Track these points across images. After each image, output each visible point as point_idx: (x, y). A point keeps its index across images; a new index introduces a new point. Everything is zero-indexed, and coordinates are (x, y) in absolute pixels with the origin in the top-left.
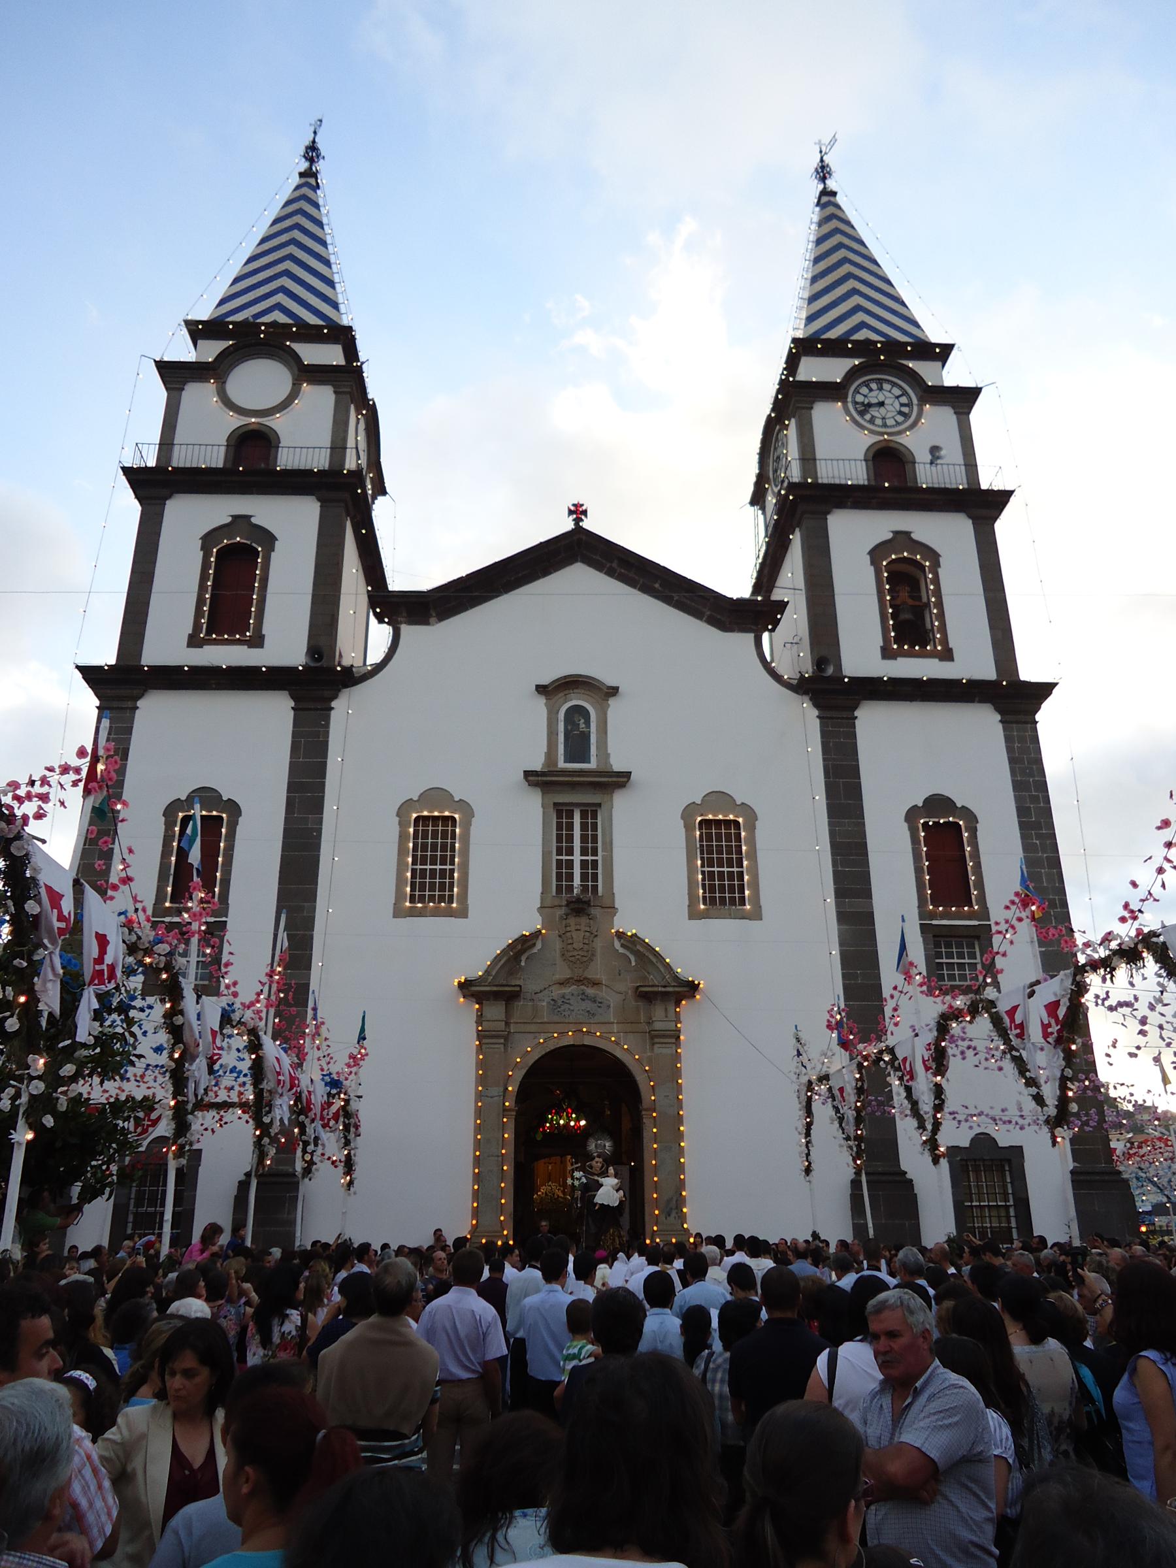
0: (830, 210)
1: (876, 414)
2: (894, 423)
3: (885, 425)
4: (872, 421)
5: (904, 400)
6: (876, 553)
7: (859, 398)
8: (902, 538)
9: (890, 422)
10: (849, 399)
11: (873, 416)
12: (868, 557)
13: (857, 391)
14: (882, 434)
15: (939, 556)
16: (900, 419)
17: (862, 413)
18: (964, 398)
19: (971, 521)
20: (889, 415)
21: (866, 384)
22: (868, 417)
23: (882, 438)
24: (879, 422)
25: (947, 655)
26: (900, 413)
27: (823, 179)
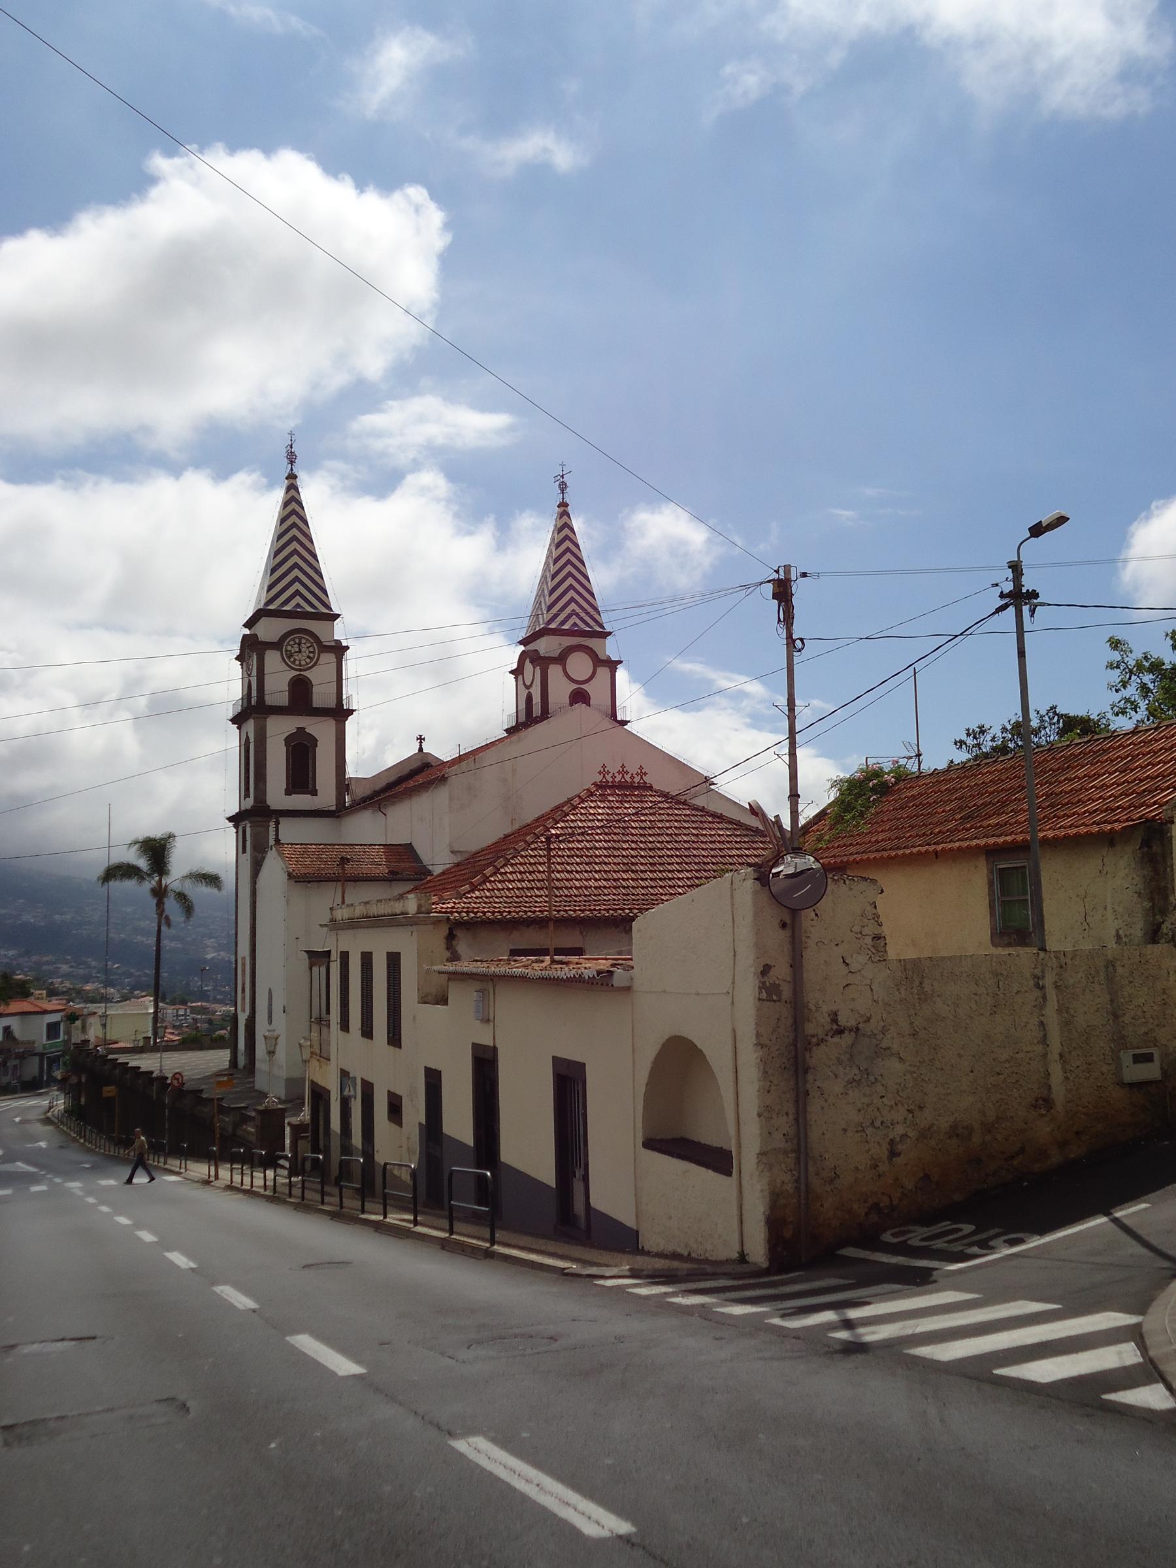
0: (293, 492)
1: (297, 658)
2: (305, 663)
3: (300, 665)
4: (294, 662)
5: (311, 649)
6: (288, 740)
7: (289, 648)
8: (301, 730)
9: (303, 663)
10: (284, 650)
11: (295, 659)
12: (284, 742)
13: (288, 644)
14: (300, 670)
15: (317, 741)
16: (308, 660)
17: (289, 657)
18: (339, 650)
19: (335, 722)
20: (304, 658)
21: (293, 640)
22: (292, 659)
23: (298, 673)
24: (297, 663)
25: (314, 793)
26: (309, 657)
27: (292, 463)
